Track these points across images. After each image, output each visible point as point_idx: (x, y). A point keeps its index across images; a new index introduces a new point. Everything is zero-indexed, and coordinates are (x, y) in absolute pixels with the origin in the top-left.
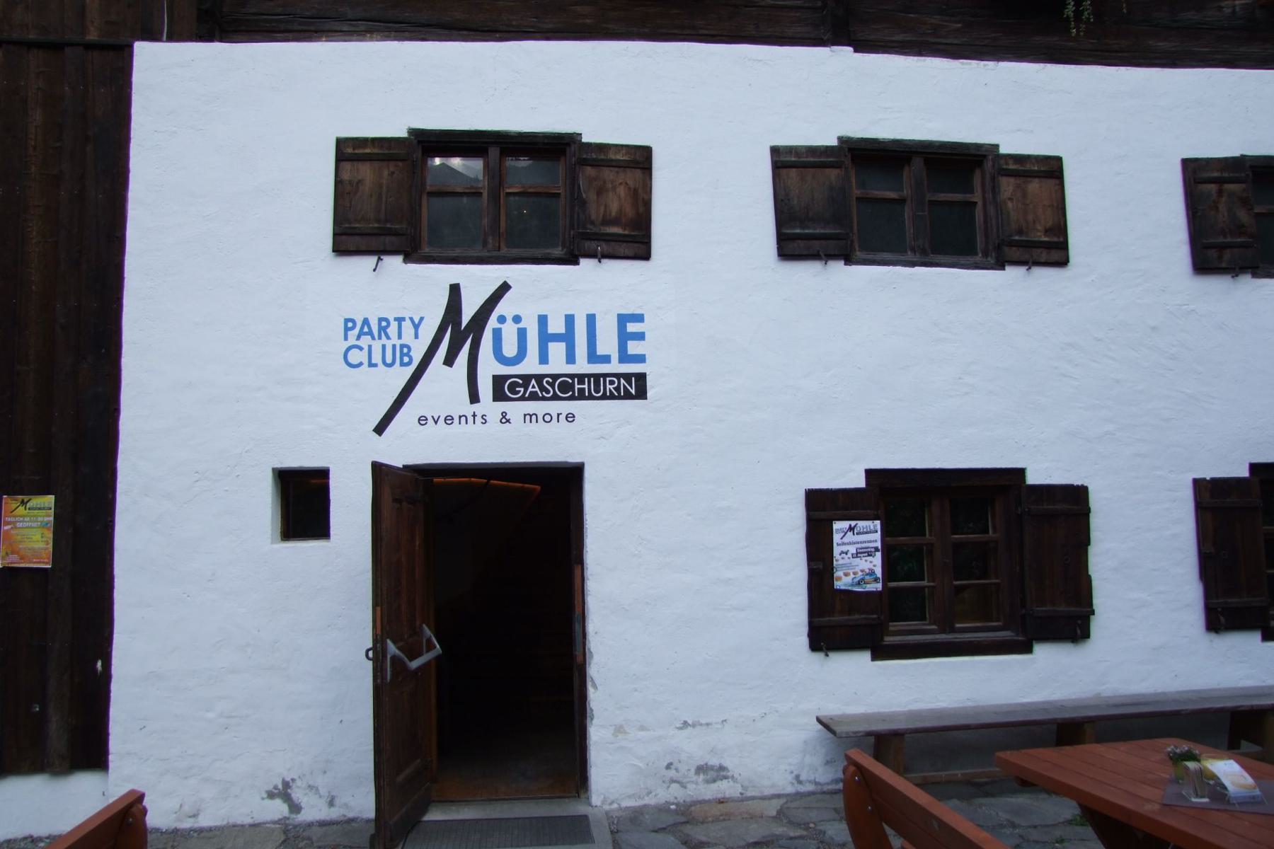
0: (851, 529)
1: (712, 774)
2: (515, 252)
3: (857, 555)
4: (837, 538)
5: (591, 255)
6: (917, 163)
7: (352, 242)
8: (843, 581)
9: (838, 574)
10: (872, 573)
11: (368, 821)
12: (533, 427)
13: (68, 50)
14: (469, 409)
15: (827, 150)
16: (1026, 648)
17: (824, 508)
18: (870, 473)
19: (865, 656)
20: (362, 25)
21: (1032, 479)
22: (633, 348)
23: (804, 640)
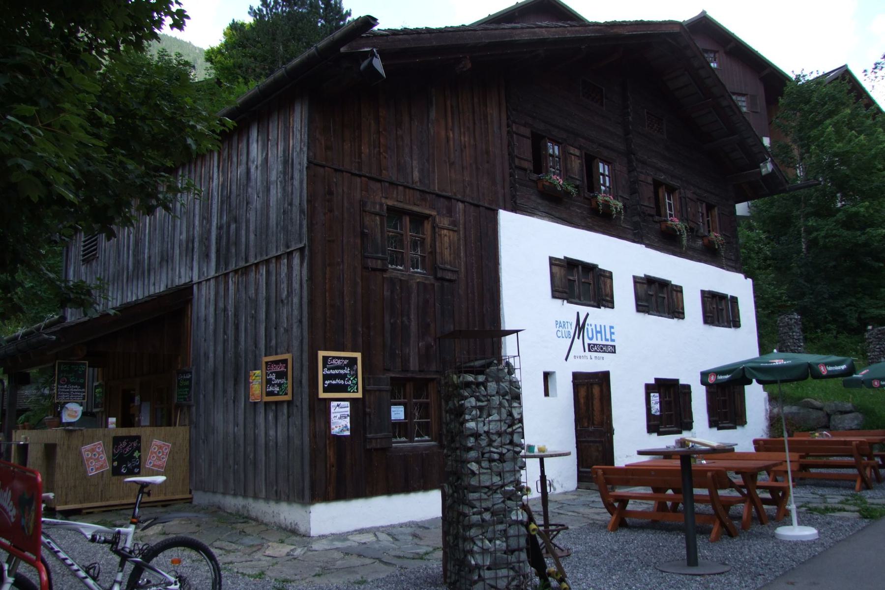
0: (338, 405)
1: (263, 527)
2: (589, 303)
3: (340, 418)
4: (332, 410)
5: (605, 307)
6: (657, 285)
7: (557, 294)
8: (653, 412)
9: (333, 426)
10: (346, 426)
11: (538, 498)
12: (597, 361)
13: (481, 208)
14: (583, 354)
15: (641, 278)
16: (734, 428)
17: (649, 389)
18: (656, 380)
19: (655, 435)
20: (544, 214)
21: (681, 382)
22: (613, 337)
23: (645, 429)
